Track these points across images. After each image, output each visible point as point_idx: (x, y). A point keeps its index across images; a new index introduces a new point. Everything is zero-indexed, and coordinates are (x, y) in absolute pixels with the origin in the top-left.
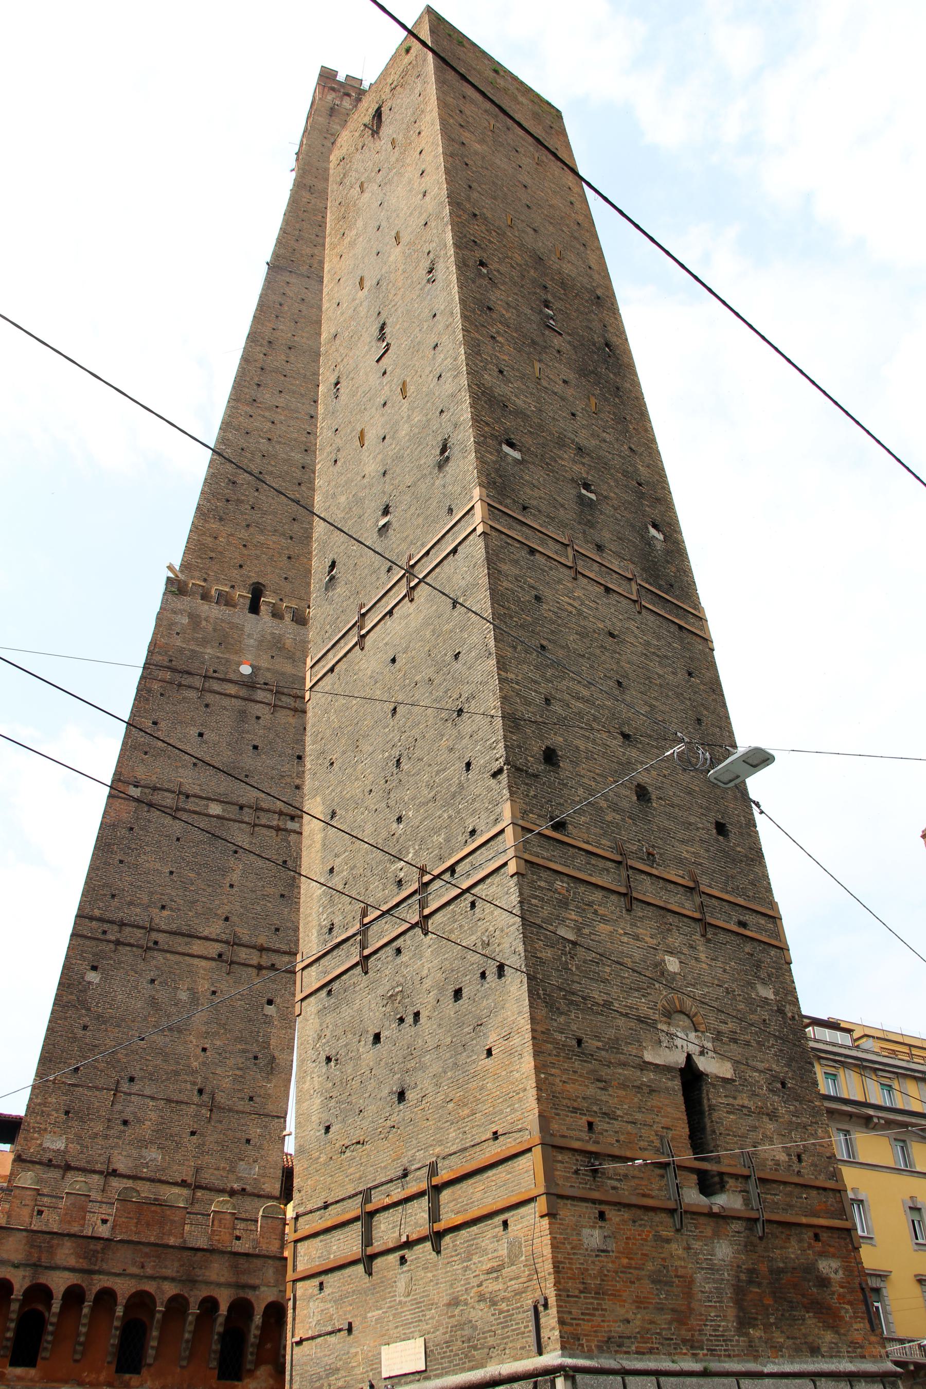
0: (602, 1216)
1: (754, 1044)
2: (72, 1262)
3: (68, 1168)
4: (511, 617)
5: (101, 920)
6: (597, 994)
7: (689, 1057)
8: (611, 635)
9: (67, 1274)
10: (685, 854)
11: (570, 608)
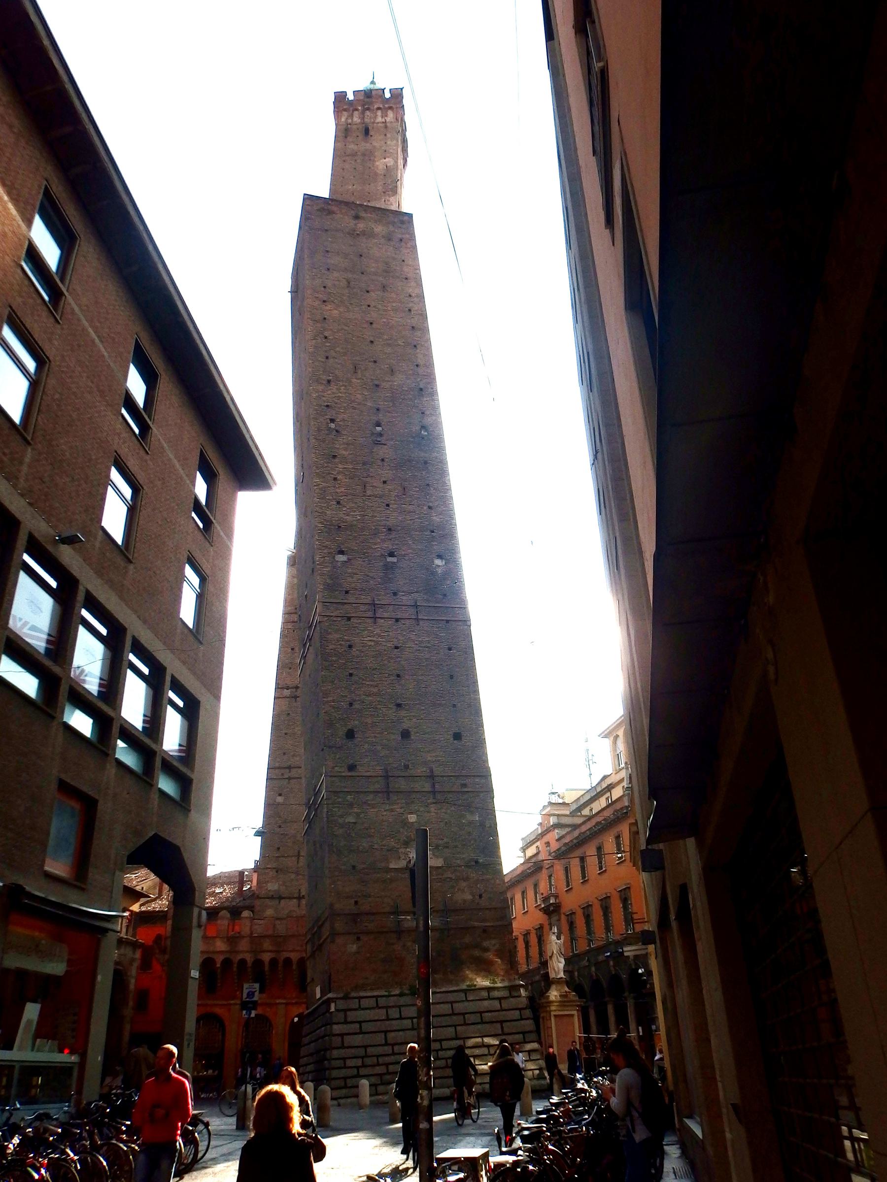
0: (358, 939)
2: (270, 948)
3: (281, 898)
4: (332, 665)
5: (279, 768)
6: (365, 844)
8: (396, 648)
9: (269, 954)
11: (370, 643)
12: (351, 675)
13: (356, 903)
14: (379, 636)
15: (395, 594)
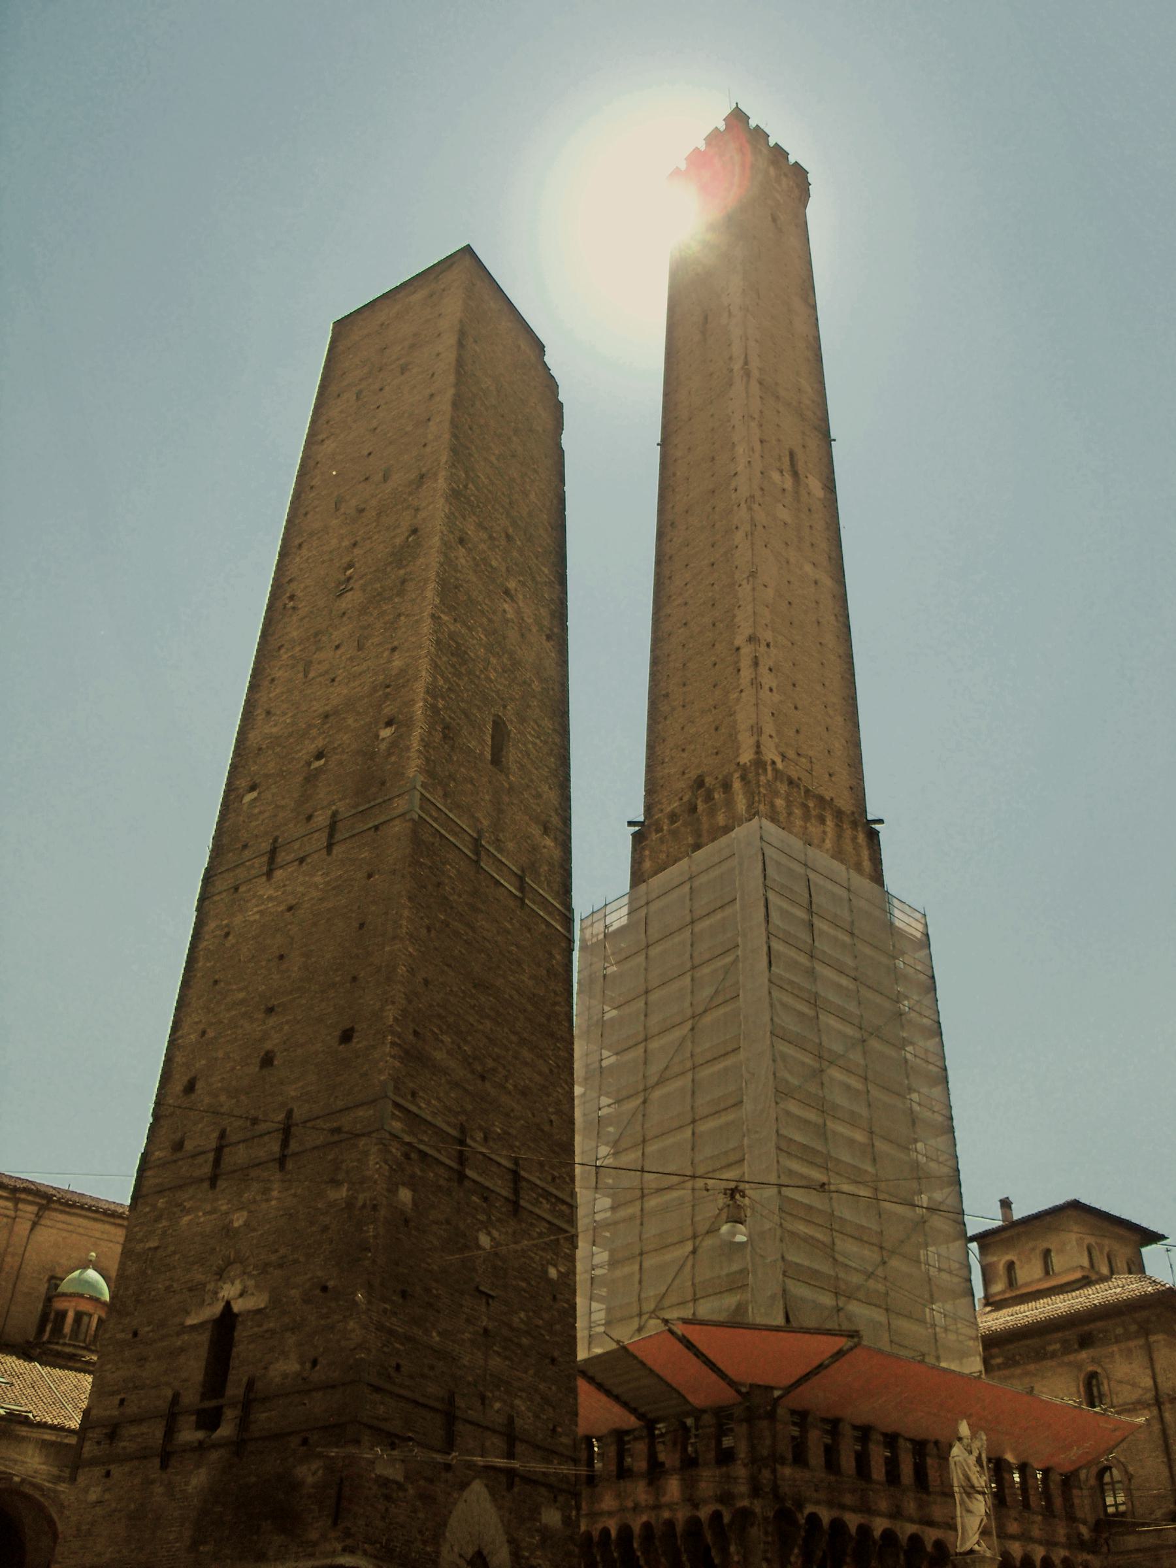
0: (108, 1474)
1: (302, 1259)
7: (228, 1304)
10: (293, 1093)
11: (252, 919)
12: (216, 982)
13: (122, 1401)
14: (270, 898)
15: (309, 818)
